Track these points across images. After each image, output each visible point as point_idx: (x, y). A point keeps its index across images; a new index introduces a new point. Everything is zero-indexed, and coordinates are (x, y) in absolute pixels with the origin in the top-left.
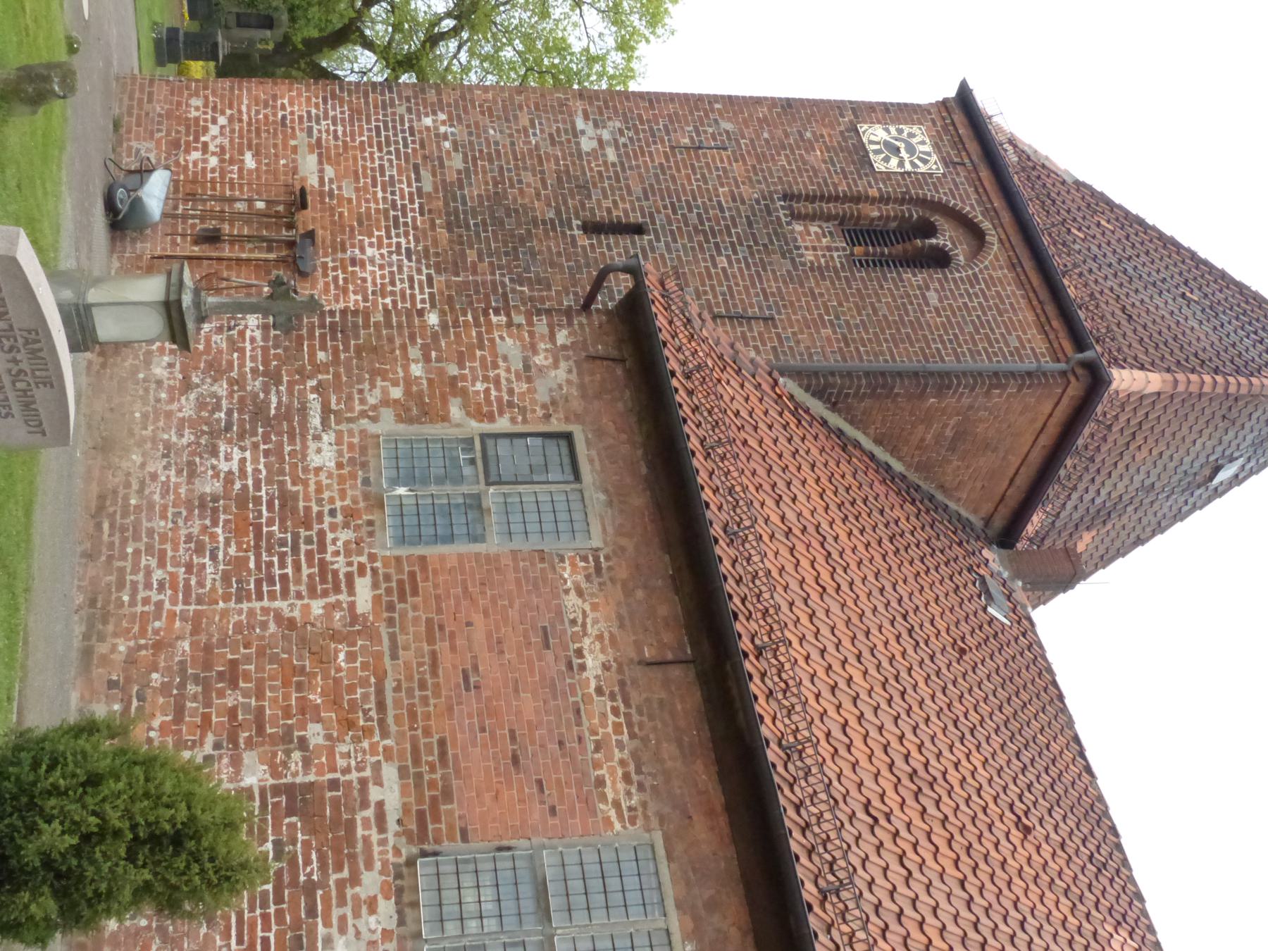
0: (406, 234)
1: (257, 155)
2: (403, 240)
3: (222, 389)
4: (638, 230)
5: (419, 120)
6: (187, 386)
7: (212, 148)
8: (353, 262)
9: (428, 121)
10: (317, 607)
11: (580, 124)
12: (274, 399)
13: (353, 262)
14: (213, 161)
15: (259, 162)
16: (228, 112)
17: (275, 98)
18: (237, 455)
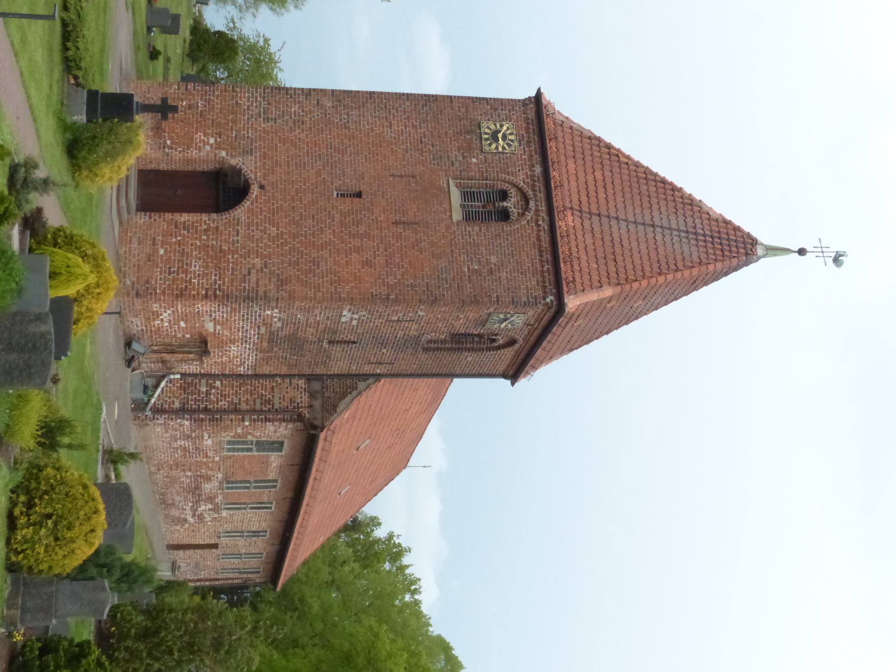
0: (250, 344)
1: (186, 322)
2: (248, 346)
3: (178, 433)
4: (354, 342)
5: (265, 311)
6: (167, 432)
7: (165, 320)
8: (226, 351)
9: (269, 313)
10: (205, 460)
11: (345, 313)
12: (193, 435)
13: (226, 351)
14: (166, 324)
15: (187, 325)
16: (172, 309)
17: (194, 305)
18: (183, 442)
